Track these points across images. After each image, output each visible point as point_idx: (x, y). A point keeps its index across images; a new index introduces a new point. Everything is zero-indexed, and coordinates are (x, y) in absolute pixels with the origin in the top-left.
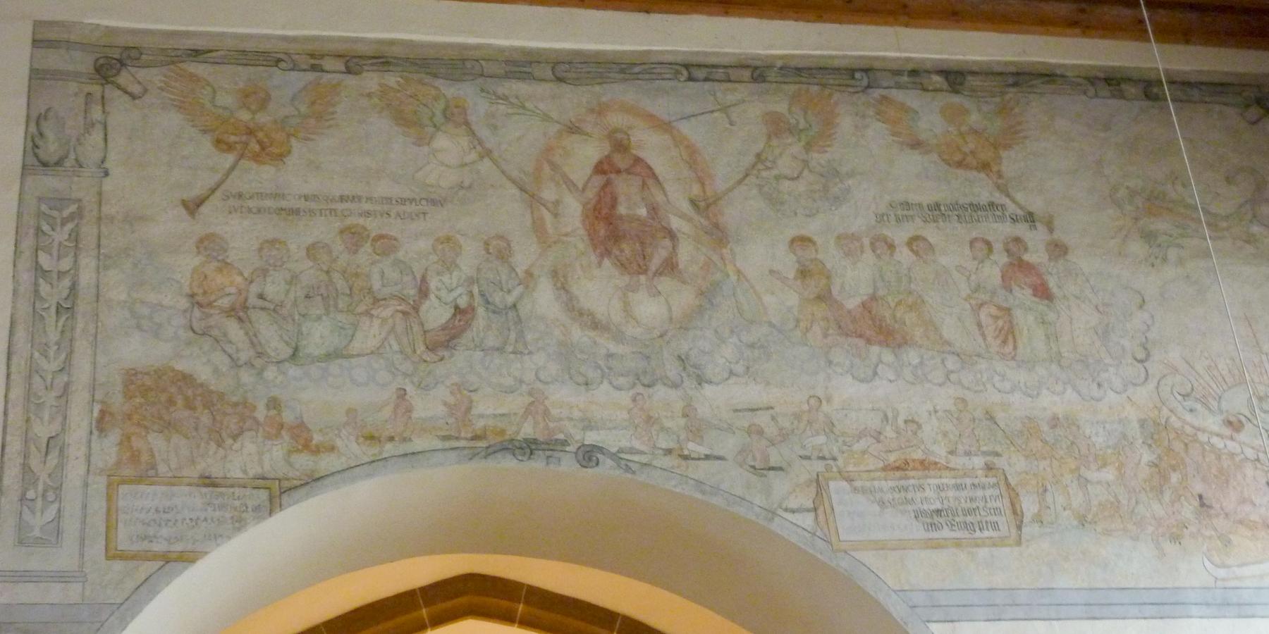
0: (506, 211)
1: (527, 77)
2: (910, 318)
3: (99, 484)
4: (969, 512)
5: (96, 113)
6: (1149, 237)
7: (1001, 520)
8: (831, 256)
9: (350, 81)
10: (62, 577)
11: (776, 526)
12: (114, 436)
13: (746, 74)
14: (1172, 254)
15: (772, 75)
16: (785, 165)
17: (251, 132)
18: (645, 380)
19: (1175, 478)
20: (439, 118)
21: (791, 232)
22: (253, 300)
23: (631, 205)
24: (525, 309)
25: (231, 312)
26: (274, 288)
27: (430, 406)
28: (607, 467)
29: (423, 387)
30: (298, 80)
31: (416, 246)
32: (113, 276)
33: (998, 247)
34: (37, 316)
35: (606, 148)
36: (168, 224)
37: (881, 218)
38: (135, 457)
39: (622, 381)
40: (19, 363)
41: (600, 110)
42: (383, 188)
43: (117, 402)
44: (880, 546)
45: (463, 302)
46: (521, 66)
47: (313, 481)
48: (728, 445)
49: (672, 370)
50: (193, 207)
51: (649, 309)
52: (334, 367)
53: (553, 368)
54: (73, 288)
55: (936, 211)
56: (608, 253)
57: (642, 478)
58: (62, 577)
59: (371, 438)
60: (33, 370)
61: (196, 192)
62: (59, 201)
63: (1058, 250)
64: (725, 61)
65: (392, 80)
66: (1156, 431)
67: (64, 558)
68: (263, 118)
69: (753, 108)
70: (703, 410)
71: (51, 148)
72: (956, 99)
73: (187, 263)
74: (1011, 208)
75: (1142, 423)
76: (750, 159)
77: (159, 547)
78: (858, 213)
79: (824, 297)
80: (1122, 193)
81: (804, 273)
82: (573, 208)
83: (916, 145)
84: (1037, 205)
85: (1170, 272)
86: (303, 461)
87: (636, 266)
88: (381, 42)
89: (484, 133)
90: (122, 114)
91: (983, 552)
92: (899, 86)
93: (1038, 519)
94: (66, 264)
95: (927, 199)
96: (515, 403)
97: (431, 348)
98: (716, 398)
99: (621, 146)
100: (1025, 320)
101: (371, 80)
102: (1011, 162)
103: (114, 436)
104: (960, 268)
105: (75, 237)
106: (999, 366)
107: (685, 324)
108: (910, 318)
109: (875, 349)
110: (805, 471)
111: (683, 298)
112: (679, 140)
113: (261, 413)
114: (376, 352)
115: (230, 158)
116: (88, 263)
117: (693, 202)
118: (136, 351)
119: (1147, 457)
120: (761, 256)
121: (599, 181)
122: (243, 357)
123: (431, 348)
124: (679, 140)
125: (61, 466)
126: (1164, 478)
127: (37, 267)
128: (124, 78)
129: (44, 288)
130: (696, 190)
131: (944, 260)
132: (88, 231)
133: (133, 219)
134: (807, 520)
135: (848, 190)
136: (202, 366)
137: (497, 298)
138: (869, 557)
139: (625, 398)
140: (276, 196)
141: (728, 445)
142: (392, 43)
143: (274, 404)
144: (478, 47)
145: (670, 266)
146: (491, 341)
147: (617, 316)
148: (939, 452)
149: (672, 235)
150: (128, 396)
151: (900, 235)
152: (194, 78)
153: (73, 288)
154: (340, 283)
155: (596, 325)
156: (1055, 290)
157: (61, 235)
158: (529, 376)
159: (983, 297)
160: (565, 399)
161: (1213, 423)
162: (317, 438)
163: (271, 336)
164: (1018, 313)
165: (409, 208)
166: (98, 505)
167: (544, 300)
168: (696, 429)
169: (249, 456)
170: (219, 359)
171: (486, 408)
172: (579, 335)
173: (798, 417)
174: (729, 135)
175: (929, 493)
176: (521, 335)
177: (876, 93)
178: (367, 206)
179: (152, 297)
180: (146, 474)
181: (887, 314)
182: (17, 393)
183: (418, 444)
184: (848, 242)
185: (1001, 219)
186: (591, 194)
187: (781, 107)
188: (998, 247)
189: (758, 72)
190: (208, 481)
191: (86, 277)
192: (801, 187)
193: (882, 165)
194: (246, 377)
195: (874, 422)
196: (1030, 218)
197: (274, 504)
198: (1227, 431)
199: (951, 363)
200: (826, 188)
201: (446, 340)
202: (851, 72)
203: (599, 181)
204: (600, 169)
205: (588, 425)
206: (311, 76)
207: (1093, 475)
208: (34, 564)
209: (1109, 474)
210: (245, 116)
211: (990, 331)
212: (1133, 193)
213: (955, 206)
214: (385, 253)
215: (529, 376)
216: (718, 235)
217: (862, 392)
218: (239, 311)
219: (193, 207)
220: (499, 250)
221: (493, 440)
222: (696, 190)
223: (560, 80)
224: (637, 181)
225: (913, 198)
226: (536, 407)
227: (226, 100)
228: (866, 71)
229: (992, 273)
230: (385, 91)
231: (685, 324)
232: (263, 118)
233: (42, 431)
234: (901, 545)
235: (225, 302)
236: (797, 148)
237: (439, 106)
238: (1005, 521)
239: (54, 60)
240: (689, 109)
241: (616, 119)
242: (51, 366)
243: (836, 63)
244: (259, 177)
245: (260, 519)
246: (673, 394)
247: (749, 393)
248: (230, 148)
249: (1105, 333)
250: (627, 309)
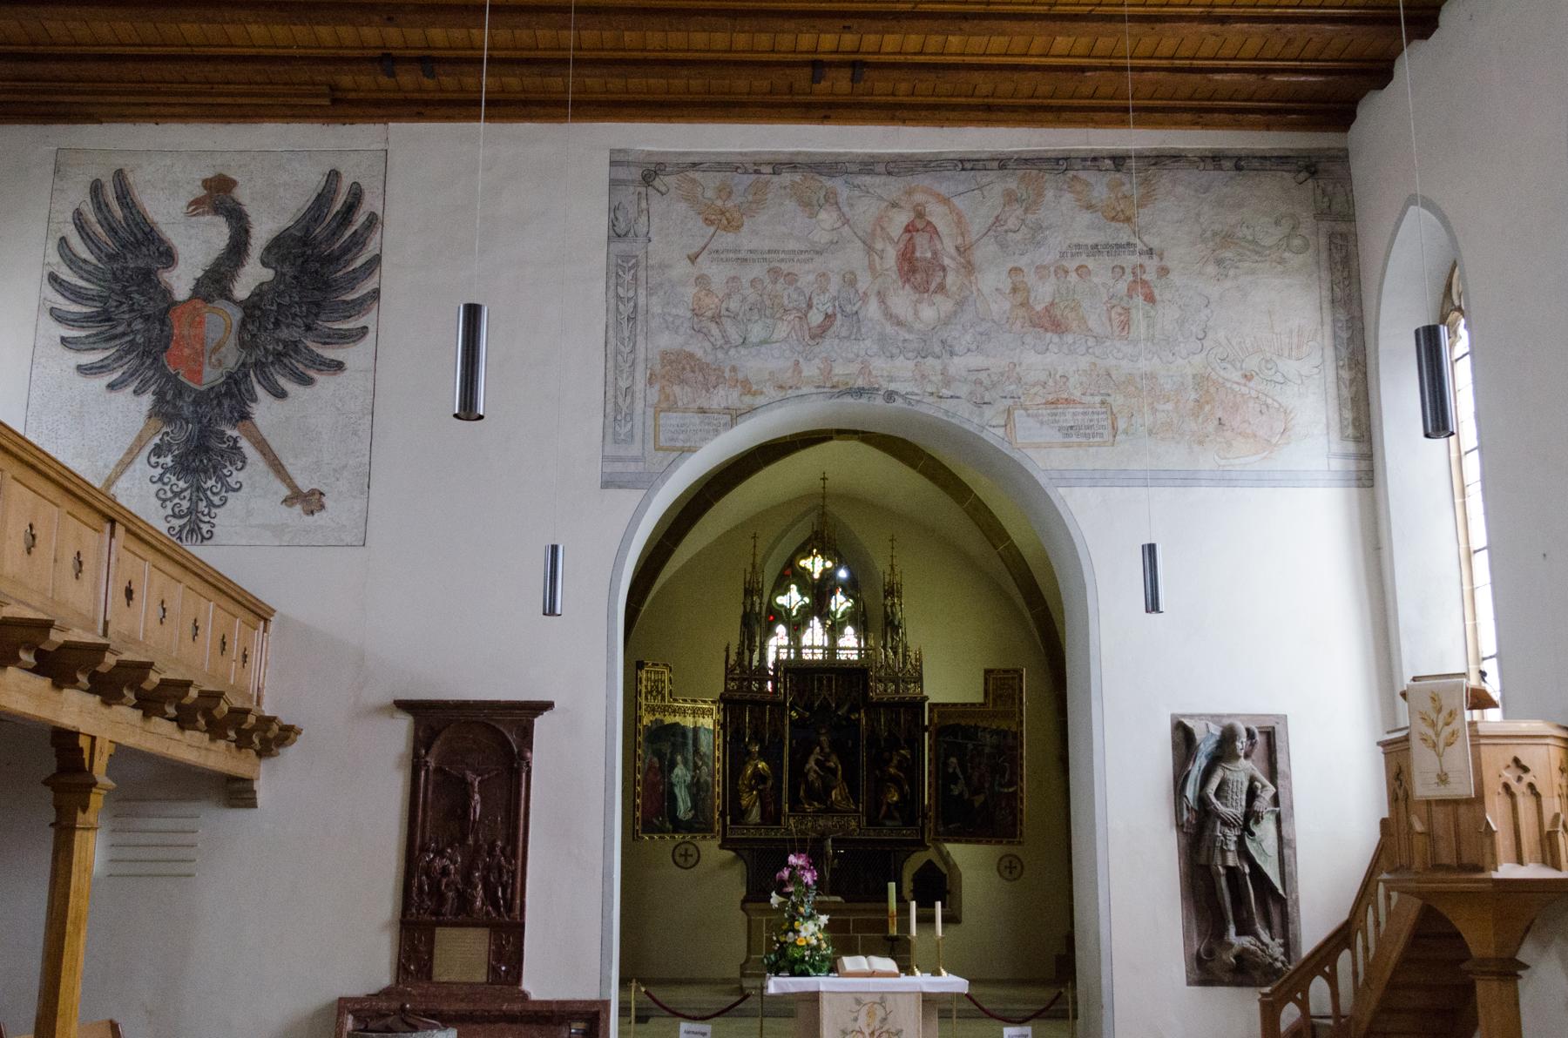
0: (854, 256)
1: (870, 172)
2: (1072, 315)
3: (650, 412)
4: (1088, 427)
5: (644, 205)
6: (1219, 262)
7: (1105, 432)
8: (1031, 278)
9: (775, 179)
10: (635, 460)
11: (983, 435)
12: (657, 387)
13: (995, 164)
14: (1231, 272)
15: (1011, 165)
16: (1012, 223)
17: (723, 213)
18: (923, 354)
19: (1207, 408)
20: (822, 201)
21: (1010, 265)
22: (724, 312)
23: (923, 252)
24: (861, 316)
25: (712, 319)
26: (734, 305)
27: (811, 370)
28: (899, 403)
29: (807, 360)
30: (749, 179)
31: (807, 280)
32: (654, 299)
33: (1128, 271)
34: (618, 323)
35: (912, 215)
36: (682, 269)
37: (1063, 255)
38: (667, 398)
39: (910, 355)
40: (611, 348)
41: (910, 193)
42: (792, 245)
43: (658, 367)
44: (1038, 446)
45: (830, 311)
46: (868, 165)
47: (752, 410)
48: (963, 390)
49: (937, 349)
50: (693, 259)
51: (928, 313)
52: (763, 349)
53: (875, 348)
54: (635, 306)
55: (1095, 249)
56: (908, 280)
57: (917, 408)
58: (635, 460)
59: (781, 387)
60: (618, 352)
61: (696, 250)
62: (626, 257)
63: (1164, 271)
64: (984, 156)
65: (798, 177)
66: (1201, 381)
67: (635, 450)
68: (729, 204)
69: (998, 185)
70: (952, 371)
71: (622, 227)
72: (1118, 175)
73: (691, 291)
74: (1140, 246)
75: (1194, 376)
76: (992, 220)
77: (679, 444)
78: (1048, 255)
79: (1025, 304)
80: (1209, 234)
81: (1015, 290)
82: (892, 254)
83: (1089, 207)
84: (1154, 242)
85: (1228, 284)
86: (748, 399)
87: (922, 289)
88: (792, 154)
89: (845, 209)
90: (657, 205)
91: (1091, 450)
92: (1084, 169)
93: (1126, 432)
94: (631, 294)
95: (1090, 242)
96: (854, 368)
97: (813, 337)
98: (958, 365)
99: (920, 215)
100: (1138, 316)
101: (787, 178)
102: (1144, 216)
103: (657, 387)
104: (1104, 285)
105: (635, 277)
106: (1118, 344)
107: (946, 322)
108: (1072, 315)
109: (1049, 335)
110: (1004, 404)
111: (945, 305)
112: (952, 209)
113: (727, 375)
114: (785, 340)
115: (712, 229)
116: (642, 292)
117: (957, 248)
118: (666, 341)
119: (1193, 396)
120: (992, 279)
121: (907, 236)
122: (720, 342)
123: (813, 337)
124: (952, 209)
125: (632, 402)
126: (1201, 408)
127: (618, 296)
128: (657, 183)
129: (621, 307)
130: (960, 240)
131: (1095, 280)
132: (642, 274)
133: (663, 266)
134: (1000, 432)
135: (1045, 238)
136: (698, 348)
137: (848, 309)
138: (1030, 452)
139: (911, 364)
140: (736, 251)
141: (963, 390)
142: (799, 153)
143: (734, 369)
144: (846, 154)
145: (941, 288)
146: (844, 333)
147: (910, 318)
148: (1077, 394)
149: (944, 269)
150: (664, 367)
151: (1072, 265)
152: (694, 181)
153: (635, 306)
154: (768, 303)
155: (900, 323)
156: (1158, 297)
157: (628, 277)
158: (862, 353)
159: (1114, 302)
160: (879, 365)
161: (1236, 376)
162: (754, 387)
163: (734, 334)
164: (1133, 311)
165: (806, 256)
166: (650, 422)
167: (873, 309)
168: (947, 382)
169: (723, 397)
170: (707, 345)
171: (839, 370)
172: (890, 329)
173: (1002, 374)
174: (980, 204)
175: (1069, 417)
176: (859, 329)
177: (1071, 174)
178: (782, 256)
179: (674, 311)
180: (672, 408)
181: (1058, 313)
182: (610, 364)
183: (805, 390)
184: (1041, 269)
185: (1133, 253)
186: (901, 245)
187: (1013, 186)
188: (1128, 271)
189: (1003, 163)
190: (702, 411)
191: (642, 301)
192: (1018, 236)
193: (1067, 217)
194: (720, 355)
195: (1043, 377)
196: (1150, 252)
197: (733, 423)
198: (1243, 381)
199: (1091, 342)
200: (1033, 237)
201: (820, 333)
202: (1057, 160)
203: (907, 236)
204: (907, 230)
205: (891, 379)
206: (754, 177)
207: (1160, 407)
208: (622, 453)
209: (1169, 406)
210: (719, 203)
211: (1115, 323)
212: (1215, 234)
213: (1107, 246)
214: (791, 283)
215: (862, 353)
216: (969, 268)
217: (1041, 360)
218: (716, 319)
219: (693, 259)
220: (850, 281)
221: (842, 388)
222: (960, 240)
223: (890, 173)
224: (927, 236)
225: (1083, 241)
226: (865, 370)
227: (709, 194)
228: (1066, 159)
229: (1122, 287)
230: (793, 184)
231: (946, 322)
232: (729, 204)
233: (623, 384)
234: (1050, 446)
235: (709, 314)
236: (1019, 212)
237: (823, 193)
238: (1107, 433)
239: (622, 173)
240: (961, 189)
241: (919, 197)
242: (628, 350)
243: (1049, 155)
244: (726, 239)
245: (726, 430)
246: (937, 364)
247: (975, 361)
248: (712, 223)
249: (1181, 322)
250: (916, 313)
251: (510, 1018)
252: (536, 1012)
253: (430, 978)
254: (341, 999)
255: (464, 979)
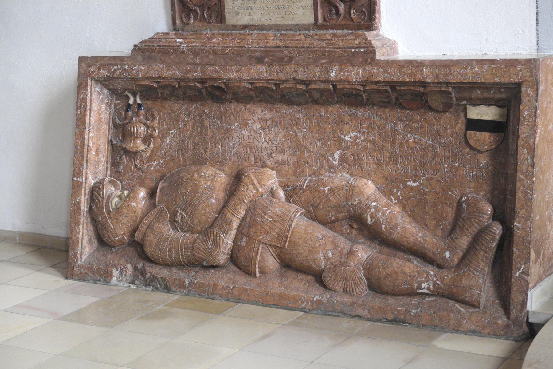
251: (352, 97)
252: (393, 86)
253: (221, 19)
254: (81, 59)
255: (276, 19)
